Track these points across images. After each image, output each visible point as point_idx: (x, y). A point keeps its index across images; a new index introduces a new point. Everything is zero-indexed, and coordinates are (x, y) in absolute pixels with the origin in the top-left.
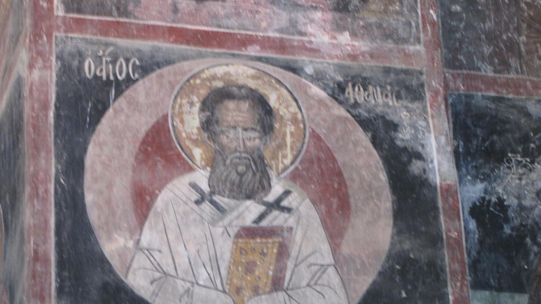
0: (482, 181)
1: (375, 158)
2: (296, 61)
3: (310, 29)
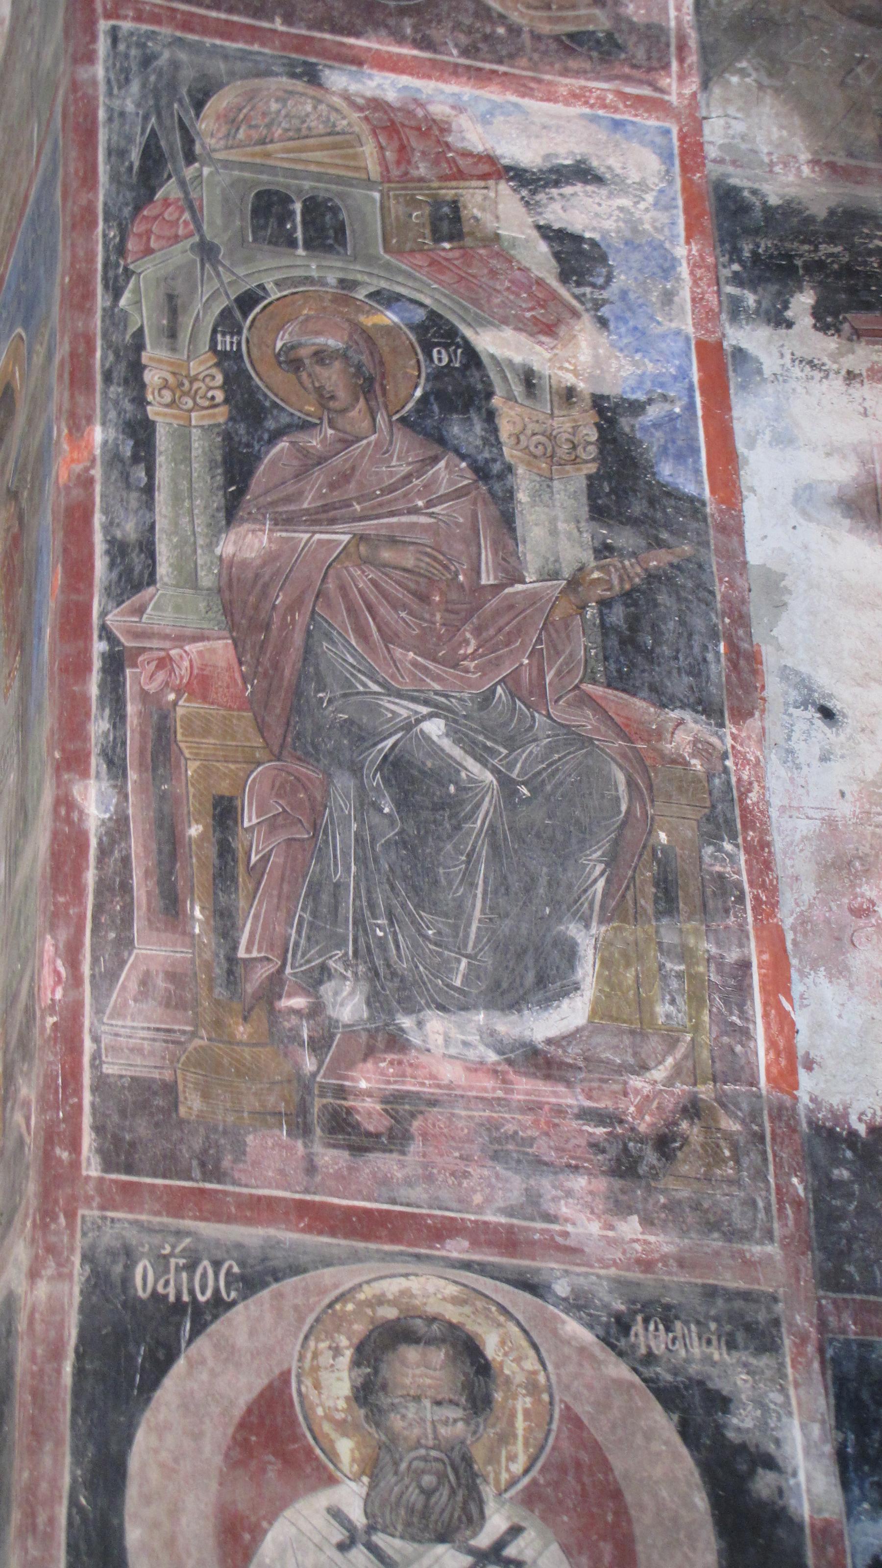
1: (685, 1466)
2: (538, 1271)
3: (564, 1210)
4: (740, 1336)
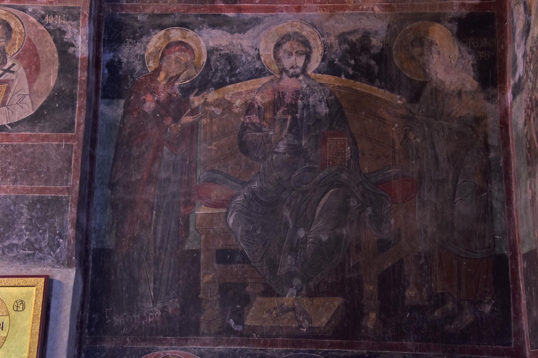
0: (113, 52)
2: (25, 6)
4: (70, 17)
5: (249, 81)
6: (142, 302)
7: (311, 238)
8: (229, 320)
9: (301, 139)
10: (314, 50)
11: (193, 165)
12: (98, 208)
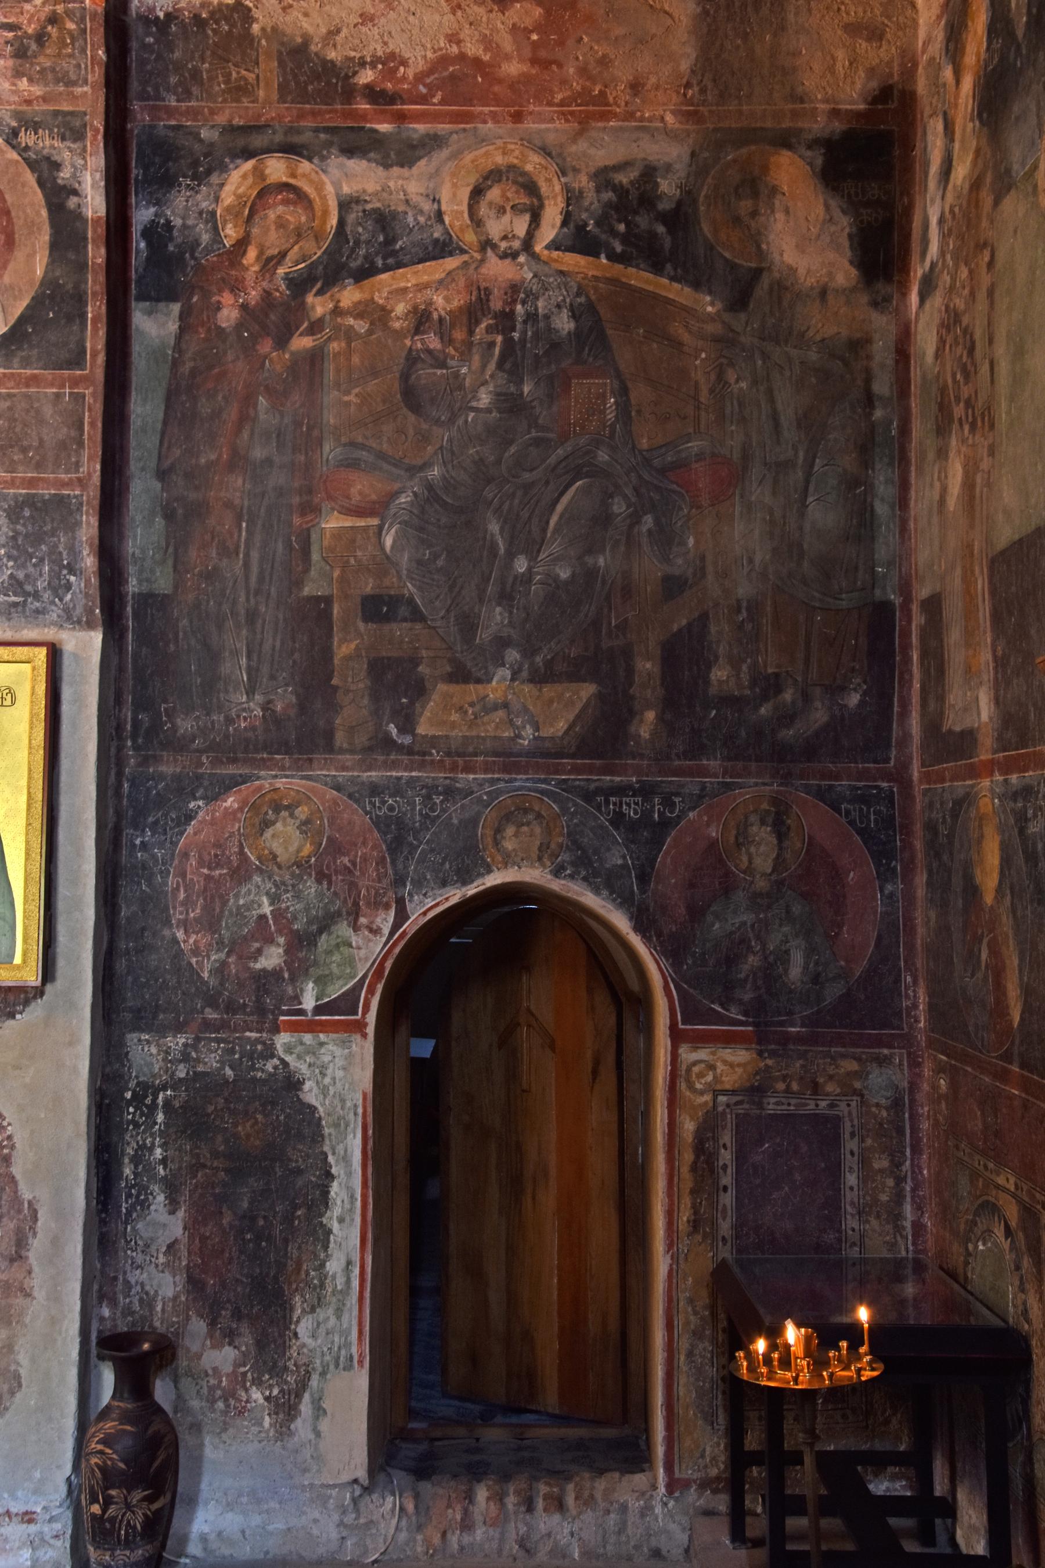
0: (154, 205)
1: (38, 196)
4: (68, 133)
5: (420, 266)
6: (227, 692)
7: (539, 573)
8: (387, 724)
9: (522, 381)
10: (546, 202)
11: (316, 433)
12: (139, 518)
